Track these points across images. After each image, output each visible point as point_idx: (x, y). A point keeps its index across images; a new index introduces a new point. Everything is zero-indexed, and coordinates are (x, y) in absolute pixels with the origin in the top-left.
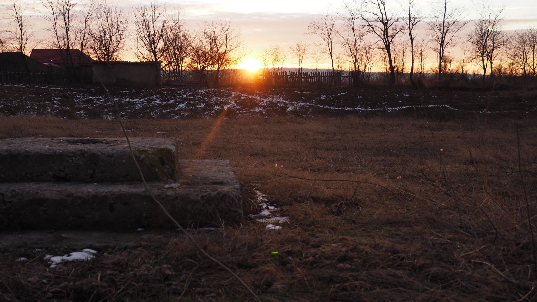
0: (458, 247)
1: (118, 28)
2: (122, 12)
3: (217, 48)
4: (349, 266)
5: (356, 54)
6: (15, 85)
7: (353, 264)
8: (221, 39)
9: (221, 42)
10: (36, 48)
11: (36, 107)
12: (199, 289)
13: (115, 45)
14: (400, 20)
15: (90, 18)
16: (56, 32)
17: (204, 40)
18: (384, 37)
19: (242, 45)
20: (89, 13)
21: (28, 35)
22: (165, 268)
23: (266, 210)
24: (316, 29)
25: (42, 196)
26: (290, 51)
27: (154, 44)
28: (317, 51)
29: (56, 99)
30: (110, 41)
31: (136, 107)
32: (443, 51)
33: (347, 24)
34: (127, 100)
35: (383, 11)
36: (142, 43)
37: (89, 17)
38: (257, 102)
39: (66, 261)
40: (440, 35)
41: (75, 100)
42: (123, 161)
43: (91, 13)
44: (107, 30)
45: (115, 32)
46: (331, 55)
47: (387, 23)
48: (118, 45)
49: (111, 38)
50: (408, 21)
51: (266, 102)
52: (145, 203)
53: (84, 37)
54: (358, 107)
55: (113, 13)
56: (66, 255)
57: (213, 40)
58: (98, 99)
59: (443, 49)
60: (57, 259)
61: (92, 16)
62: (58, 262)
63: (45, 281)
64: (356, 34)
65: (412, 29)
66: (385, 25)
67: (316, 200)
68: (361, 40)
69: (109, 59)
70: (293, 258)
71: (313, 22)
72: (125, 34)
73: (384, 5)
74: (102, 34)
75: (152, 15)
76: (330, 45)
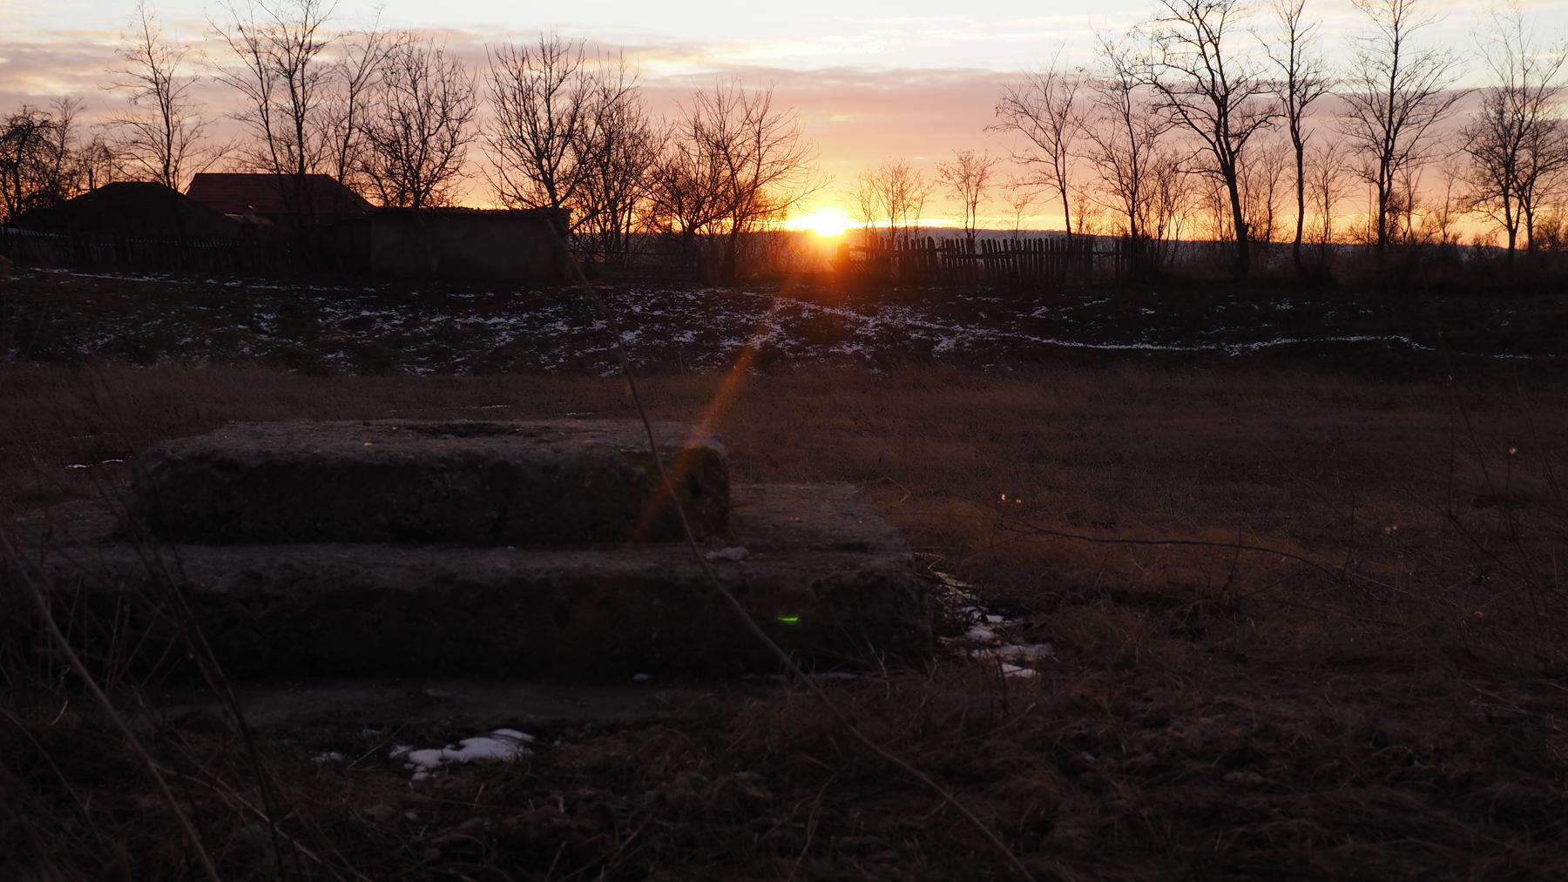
0: (1555, 727)
1: (444, 113)
2: (457, 68)
3: (732, 169)
4: (1258, 779)
5: (1137, 187)
6: (147, 278)
7: (1267, 772)
8: (742, 144)
9: (744, 153)
10: (208, 171)
11: (208, 342)
12: (848, 839)
13: (438, 161)
14: (1263, 88)
15: (367, 83)
16: (267, 124)
17: (694, 148)
18: (1218, 139)
19: (802, 160)
20: (362, 69)
21: (186, 132)
22: (743, 781)
23: (981, 624)
24: (1018, 116)
25: (368, 581)
26: (940, 179)
27: (549, 161)
28: (1022, 179)
29: (265, 317)
30: (422, 151)
32: (1390, 178)
33: (1109, 102)
34: (472, 320)
35: (1214, 64)
36: (515, 156)
37: (361, 80)
38: (848, 326)
39: (451, 761)
40: (1380, 132)
41: (320, 321)
42: (587, 485)
43: (367, 72)
44: (413, 120)
45: (438, 124)
46: (1063, 191)
47: (1225, 97)
48: (446, 161)
49: (424, 142)
50: (1288, 91)
51: (875, 327)
52: (655, 603)
53: (348, 138)
55: (432, 71)
56: (449, 746)
57: (719, 148)
58: (387, 319)
59: (1391, 171)
60: (426, 757)
61: (370, 80)
62: (431, 766)
63: (411, 815)
64: (1137, 129)
65: (1298, 114)
66: (1221, 103)
67: (1121, 597)
68: (1149, 147)
69: (417, 202)
70: (1096, 755)
72: (468, 128)
73: (1216, 45)
74: (399, 129)
75: (543, 75)
76: (1060, 160)
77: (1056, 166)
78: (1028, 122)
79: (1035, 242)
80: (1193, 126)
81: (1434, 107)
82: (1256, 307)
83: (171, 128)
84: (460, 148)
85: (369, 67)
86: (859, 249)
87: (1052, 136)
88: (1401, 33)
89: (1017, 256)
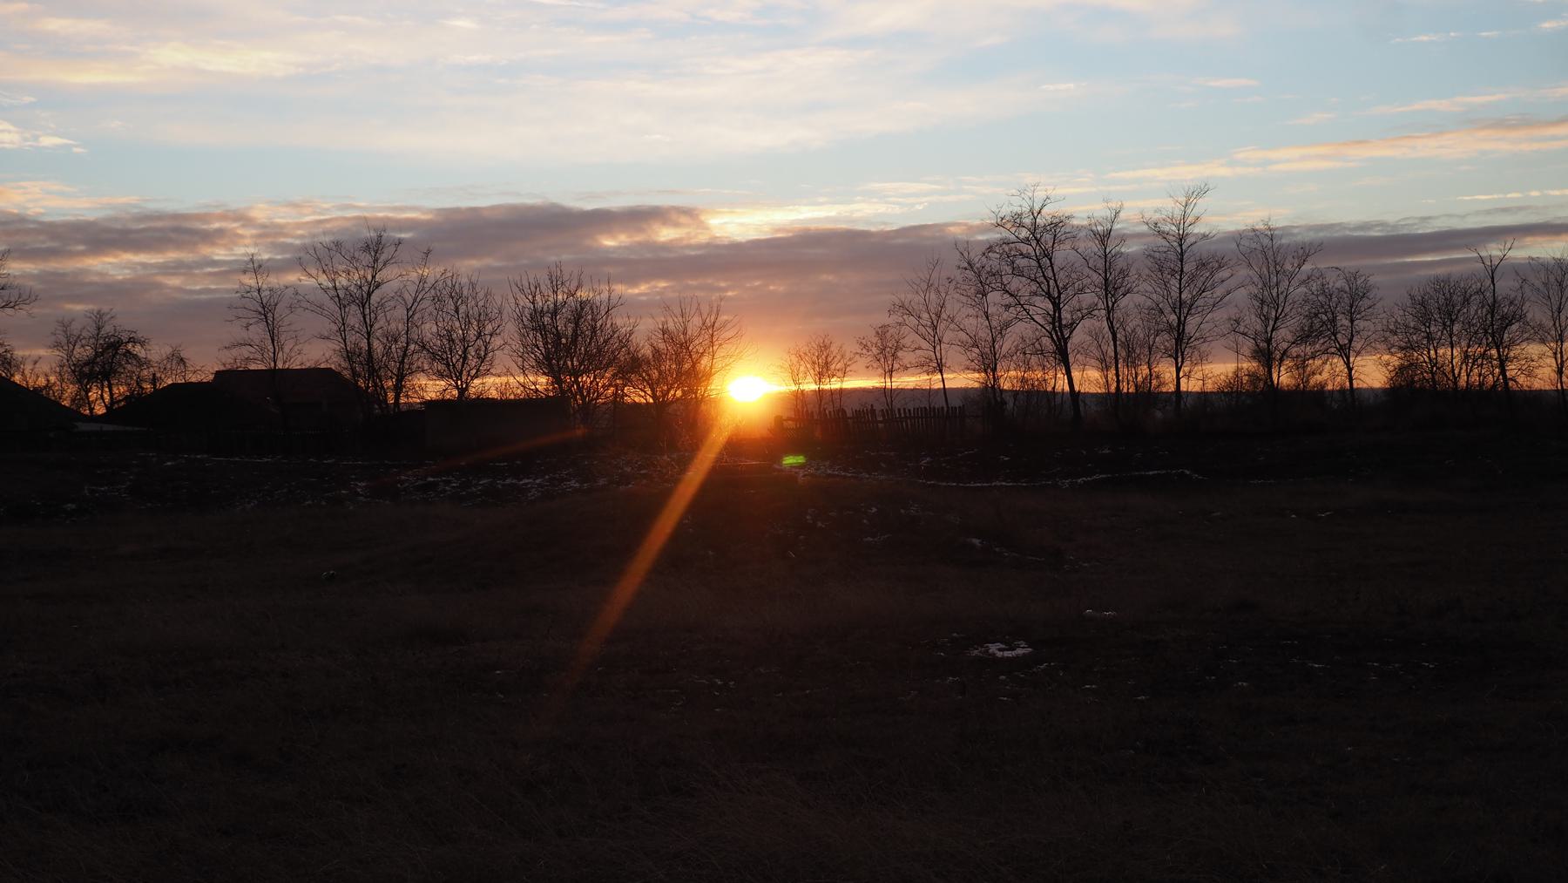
5: (996, 365)
8: (696, 346)
16: (345, 342)
18: (1054, 328)
20: (415, 300)
21: (286, 349)
24: (905, 317)
31: (529, 495)
34: (508, 481)
35: (1050, 274)
41: (399, 485)
47: (1059, 297)
54: (1000, 481)
58: (448, 483)
64: (994, 323)
68: (1003, 337)
71: (897, 302)
72: (497, 341)
73: (1050, 260)
76: (938, 348)
77: (935, 352)
78: (912, 321)
79: (921, 410)
80: (1035, 321)
81: (1212, 300)
82: (1085, 453)
83: (277, 350)
84: (490, 355)
85: (420, 297)
86: (789, 419)
87: (930, 331)
88: (1184, 247)
89: (909, 421)
